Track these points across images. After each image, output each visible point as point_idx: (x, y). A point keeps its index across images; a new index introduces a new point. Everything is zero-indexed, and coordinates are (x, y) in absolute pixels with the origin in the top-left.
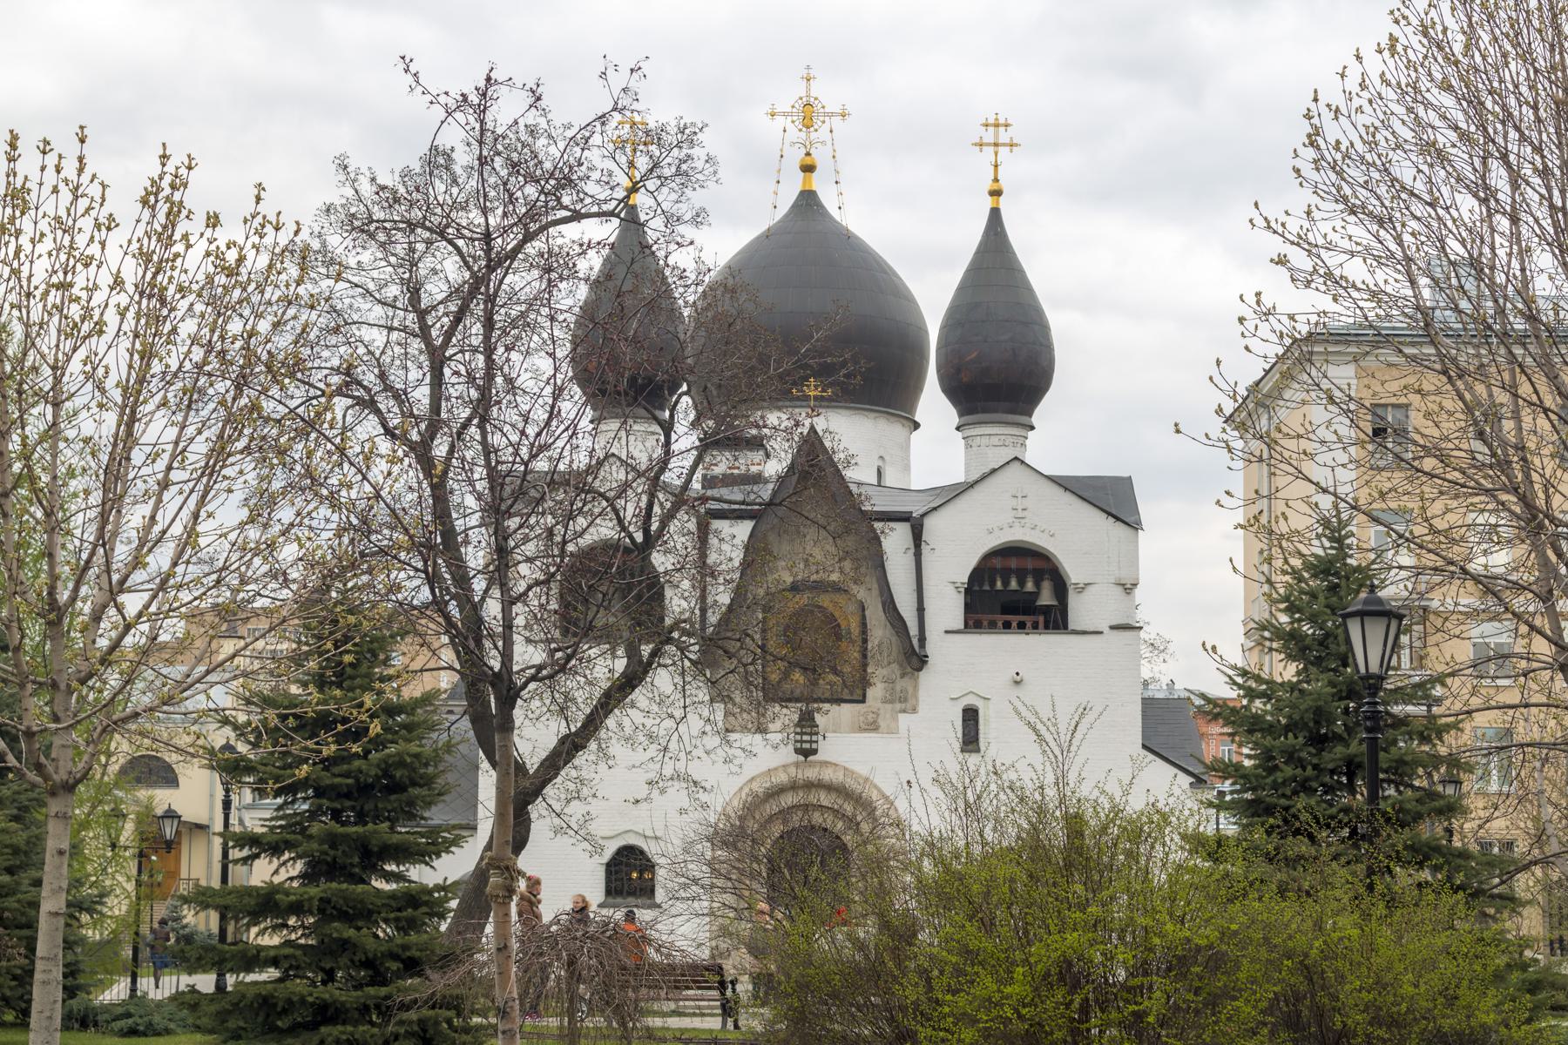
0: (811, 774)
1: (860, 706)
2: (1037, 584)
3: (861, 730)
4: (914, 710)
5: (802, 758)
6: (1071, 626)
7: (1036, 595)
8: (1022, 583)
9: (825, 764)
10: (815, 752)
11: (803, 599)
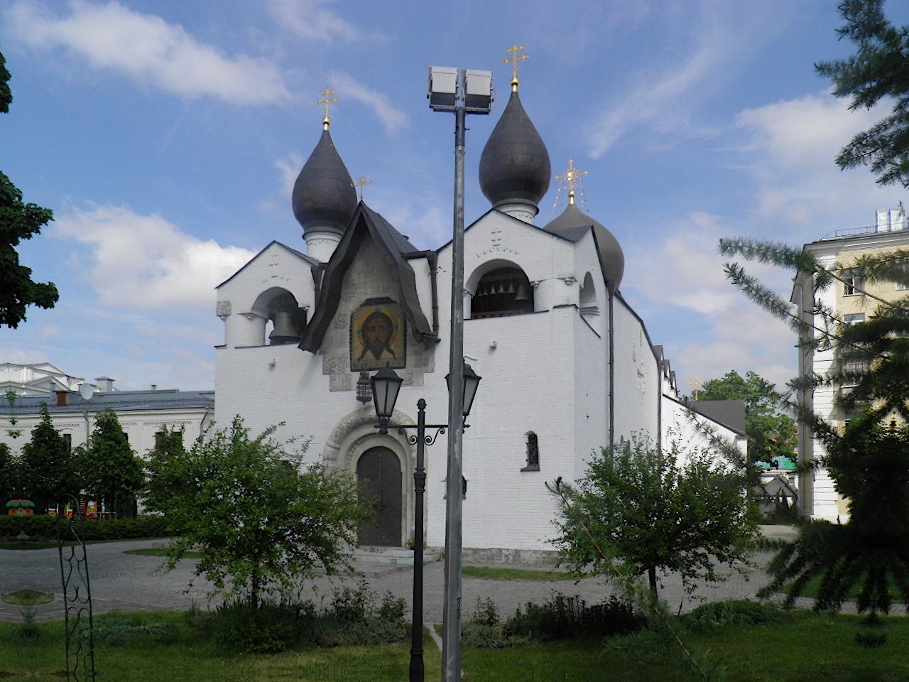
1: (403, 370)
2: (516, 289)
4: (433, 371)
6: (536, 311)
7: (515, 294)
8: (506, 289)
11: (372, 309)
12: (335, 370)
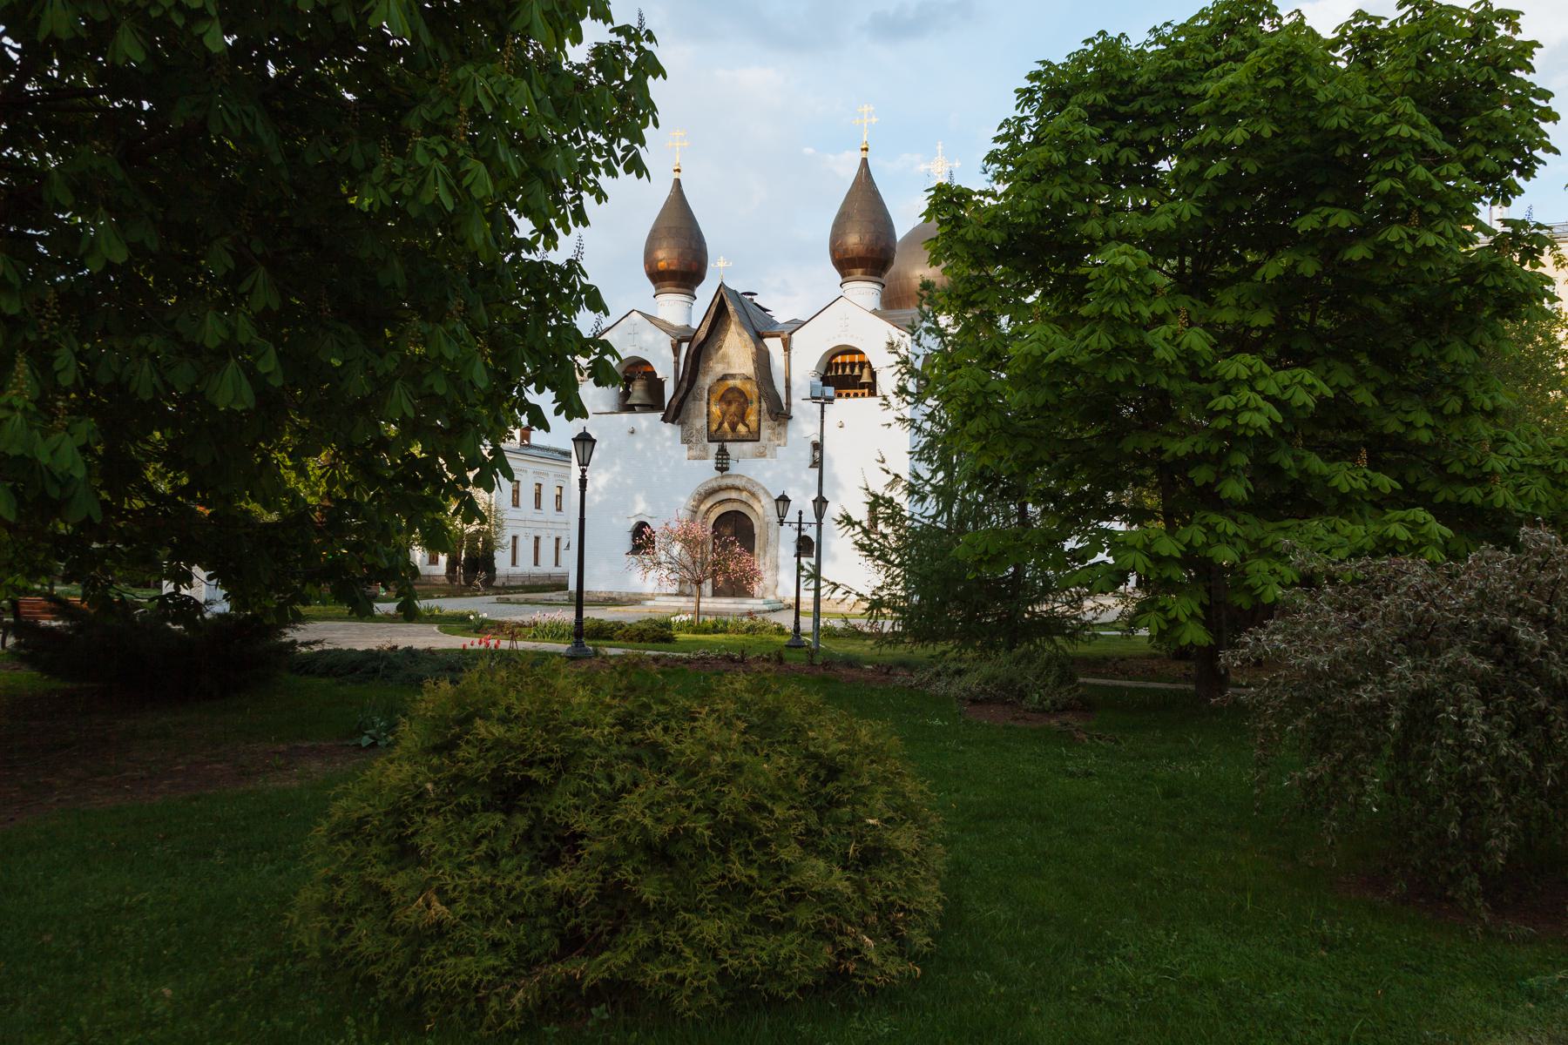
0: (729, 482)
2: (861, 370)
3: (757, 457)
5: (719, 473)
9: (737, 476)
10: (727, 469)
12: (694, 440)
